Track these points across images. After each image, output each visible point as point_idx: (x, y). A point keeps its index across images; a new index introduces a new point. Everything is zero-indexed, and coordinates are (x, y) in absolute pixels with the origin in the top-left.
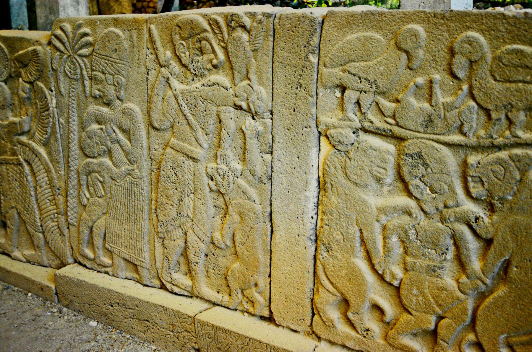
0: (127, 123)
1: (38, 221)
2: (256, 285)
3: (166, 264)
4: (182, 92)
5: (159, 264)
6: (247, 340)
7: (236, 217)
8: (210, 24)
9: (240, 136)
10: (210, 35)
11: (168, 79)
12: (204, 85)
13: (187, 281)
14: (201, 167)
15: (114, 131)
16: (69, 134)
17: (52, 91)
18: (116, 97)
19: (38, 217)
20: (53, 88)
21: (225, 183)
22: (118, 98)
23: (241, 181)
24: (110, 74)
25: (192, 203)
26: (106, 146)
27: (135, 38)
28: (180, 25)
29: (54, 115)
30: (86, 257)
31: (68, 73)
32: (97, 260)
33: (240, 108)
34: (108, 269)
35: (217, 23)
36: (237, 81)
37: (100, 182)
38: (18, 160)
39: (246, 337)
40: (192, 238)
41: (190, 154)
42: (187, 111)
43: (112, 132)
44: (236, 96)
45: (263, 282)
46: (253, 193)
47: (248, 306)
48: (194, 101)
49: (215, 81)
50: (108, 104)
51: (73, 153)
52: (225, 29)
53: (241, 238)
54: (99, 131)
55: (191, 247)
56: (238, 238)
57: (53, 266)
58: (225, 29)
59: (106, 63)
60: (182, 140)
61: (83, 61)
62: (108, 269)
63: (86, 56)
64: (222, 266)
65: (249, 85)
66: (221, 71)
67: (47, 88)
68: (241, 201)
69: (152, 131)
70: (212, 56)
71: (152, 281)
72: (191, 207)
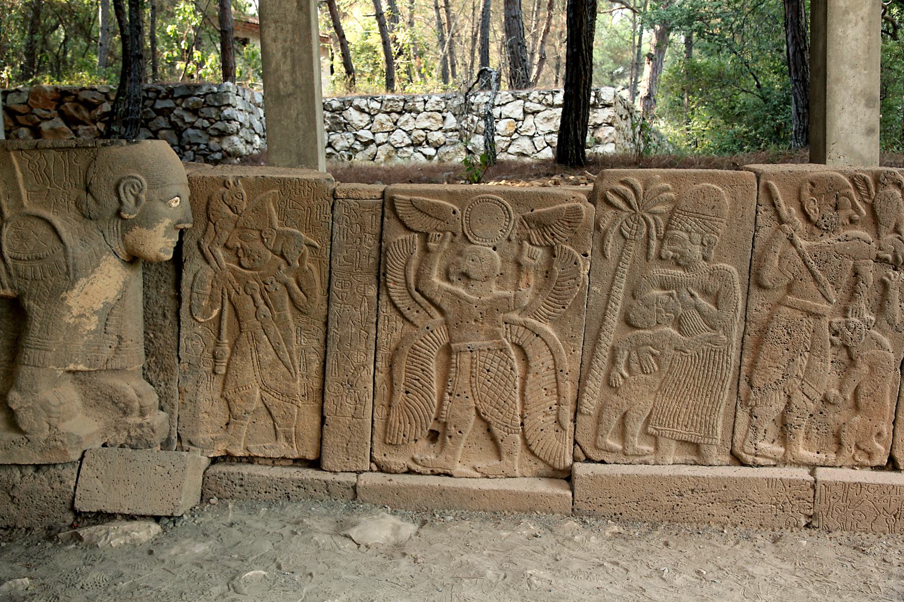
0: (714, 285)
1: (519, 419)
2: (879, 434)
3: (751, 434)
4: (808, 248)
5: (738, 436)
6: (891, 488)
7: (865, 369)
8: (853, 181)
9: (880, 288)
10: (852, 191)
11: (792, 236)
12: (839, 240)
13: (779, 450)
14: (825, 323)
15: (692, 295)
16: (608, 303)
17: (586, 255)
18: (701, 256)
19: (518, 413)
20: (589, 252)
21: (856, 336)
22: (705, 259)
23: (875, 333)
24: (697, 232)
25: (806, 362)
26: (676, 313)
27: (740, 194)
28: (814, 182)
29: (584, 282)
30: (611, 451)
31: (625, 233)
32: (630, 451)
33: (886, 260)
34: (646, 458)
35: (865, 180)
36: (883, 235)
37: (653, 355)
38: (502, 343)
39: (888, 486)
40: (798, 399)
41: (813, 310)
42: (815, 268)
43: (688, 296)
44: (880, 249)
45: (886, 428)
46: (886, 341)
47: (863, 459)
48: (825, 257)
49: (854, 236)
50: (685, 268)
51: (609, 326)
52: (872, 186)
53: (868, 389)
54: (666, 298)
55: (795, 410)
56: (864, 390)
57: (528, 474)
58: (872, 186)
59: (695, 221)
60: (804, 297)
61: (654, 219)
62: (646, 458)
63: (661, 214)
64: (832, 423)
65: (899, 238)
66: (859, 226)
67: (579, 252)
68: (874, 351)
69: (754, 291)
70: (851, 211)
71: (719, 458)
72: (804, 367)
